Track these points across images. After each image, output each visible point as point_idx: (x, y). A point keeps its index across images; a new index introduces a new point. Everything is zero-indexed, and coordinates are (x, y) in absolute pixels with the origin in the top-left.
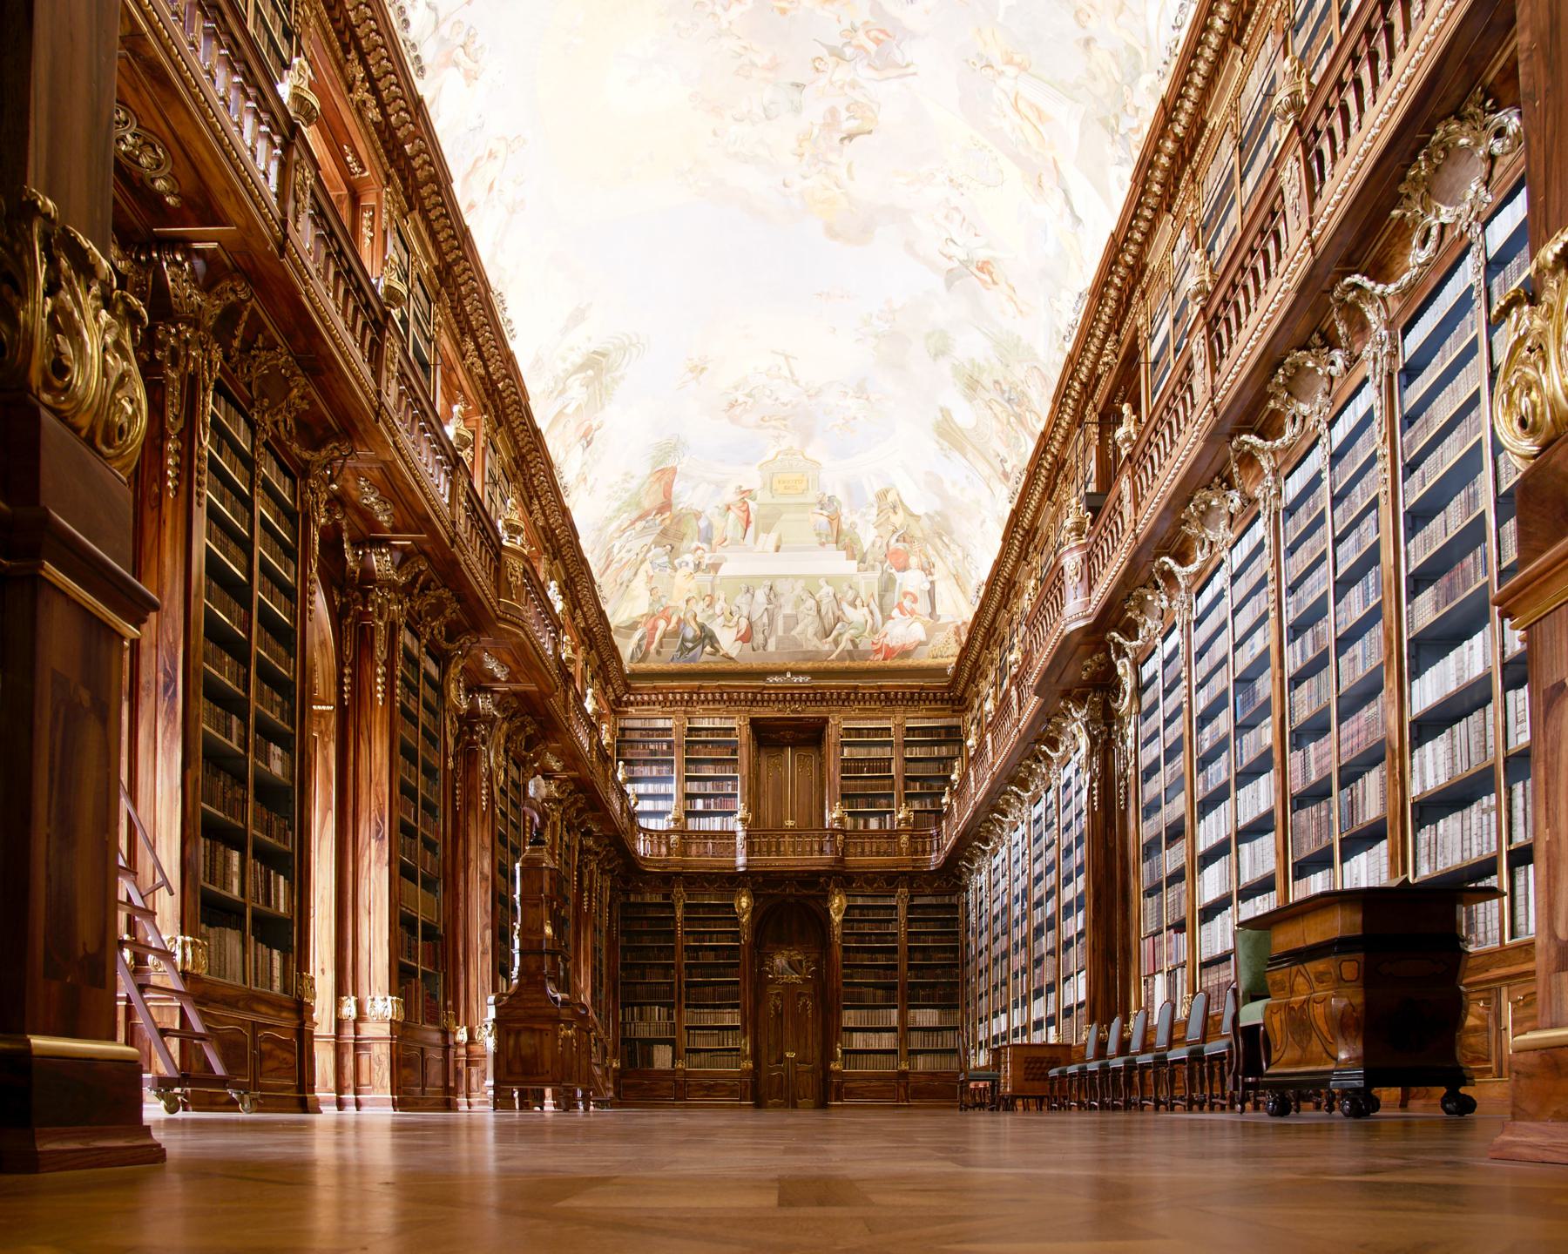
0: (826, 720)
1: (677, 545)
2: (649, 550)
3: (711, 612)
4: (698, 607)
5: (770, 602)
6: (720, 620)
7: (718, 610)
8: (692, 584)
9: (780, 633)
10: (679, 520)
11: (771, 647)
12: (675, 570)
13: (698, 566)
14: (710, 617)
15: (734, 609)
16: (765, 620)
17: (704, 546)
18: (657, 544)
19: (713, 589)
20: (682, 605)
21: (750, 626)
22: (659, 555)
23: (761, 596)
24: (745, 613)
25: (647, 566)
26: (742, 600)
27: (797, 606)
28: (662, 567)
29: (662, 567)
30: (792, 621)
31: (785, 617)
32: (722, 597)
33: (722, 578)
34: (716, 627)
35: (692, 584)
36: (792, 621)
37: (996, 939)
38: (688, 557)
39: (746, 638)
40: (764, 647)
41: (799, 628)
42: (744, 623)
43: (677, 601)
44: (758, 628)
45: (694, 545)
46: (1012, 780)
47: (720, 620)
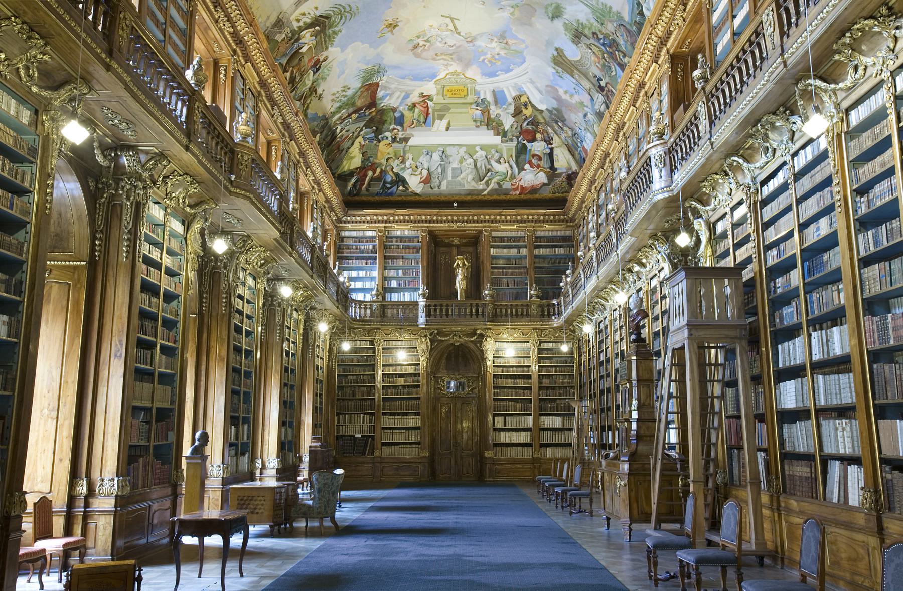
0: (481, 232)
1: (380, 127)
2: (361, 130)
4: (395, 164)
5: (442, 160)
7: (408, 164)
8: (390, 150)
9: (450, 178)
10: (382, 112)
11: (444, 187)
12: (379, 141)
13: (394, 140)
14: (402, 169)
15: (418, 164)
16: (440, 171)
17: (399, 128)
18: (366, 126)
19: (405, 152)
20: (384, 162)
21: (430, 174)
22: (368, 132)
23: (436, 157)
24: (426, 167)
26: (424, 159)
27: (461, 162)
29: (371, 140)
30: (457, 172)
31: (453, 169)
32: (411, 157)
33: (411, 147)
34: (406, 175)
36: (457, 172)
37: (602, 377)
39: (427, 181)
41: (462, 176)
42: (425, 173)
44: (434, 176)
45: (391, 127)
46: (611, 282)
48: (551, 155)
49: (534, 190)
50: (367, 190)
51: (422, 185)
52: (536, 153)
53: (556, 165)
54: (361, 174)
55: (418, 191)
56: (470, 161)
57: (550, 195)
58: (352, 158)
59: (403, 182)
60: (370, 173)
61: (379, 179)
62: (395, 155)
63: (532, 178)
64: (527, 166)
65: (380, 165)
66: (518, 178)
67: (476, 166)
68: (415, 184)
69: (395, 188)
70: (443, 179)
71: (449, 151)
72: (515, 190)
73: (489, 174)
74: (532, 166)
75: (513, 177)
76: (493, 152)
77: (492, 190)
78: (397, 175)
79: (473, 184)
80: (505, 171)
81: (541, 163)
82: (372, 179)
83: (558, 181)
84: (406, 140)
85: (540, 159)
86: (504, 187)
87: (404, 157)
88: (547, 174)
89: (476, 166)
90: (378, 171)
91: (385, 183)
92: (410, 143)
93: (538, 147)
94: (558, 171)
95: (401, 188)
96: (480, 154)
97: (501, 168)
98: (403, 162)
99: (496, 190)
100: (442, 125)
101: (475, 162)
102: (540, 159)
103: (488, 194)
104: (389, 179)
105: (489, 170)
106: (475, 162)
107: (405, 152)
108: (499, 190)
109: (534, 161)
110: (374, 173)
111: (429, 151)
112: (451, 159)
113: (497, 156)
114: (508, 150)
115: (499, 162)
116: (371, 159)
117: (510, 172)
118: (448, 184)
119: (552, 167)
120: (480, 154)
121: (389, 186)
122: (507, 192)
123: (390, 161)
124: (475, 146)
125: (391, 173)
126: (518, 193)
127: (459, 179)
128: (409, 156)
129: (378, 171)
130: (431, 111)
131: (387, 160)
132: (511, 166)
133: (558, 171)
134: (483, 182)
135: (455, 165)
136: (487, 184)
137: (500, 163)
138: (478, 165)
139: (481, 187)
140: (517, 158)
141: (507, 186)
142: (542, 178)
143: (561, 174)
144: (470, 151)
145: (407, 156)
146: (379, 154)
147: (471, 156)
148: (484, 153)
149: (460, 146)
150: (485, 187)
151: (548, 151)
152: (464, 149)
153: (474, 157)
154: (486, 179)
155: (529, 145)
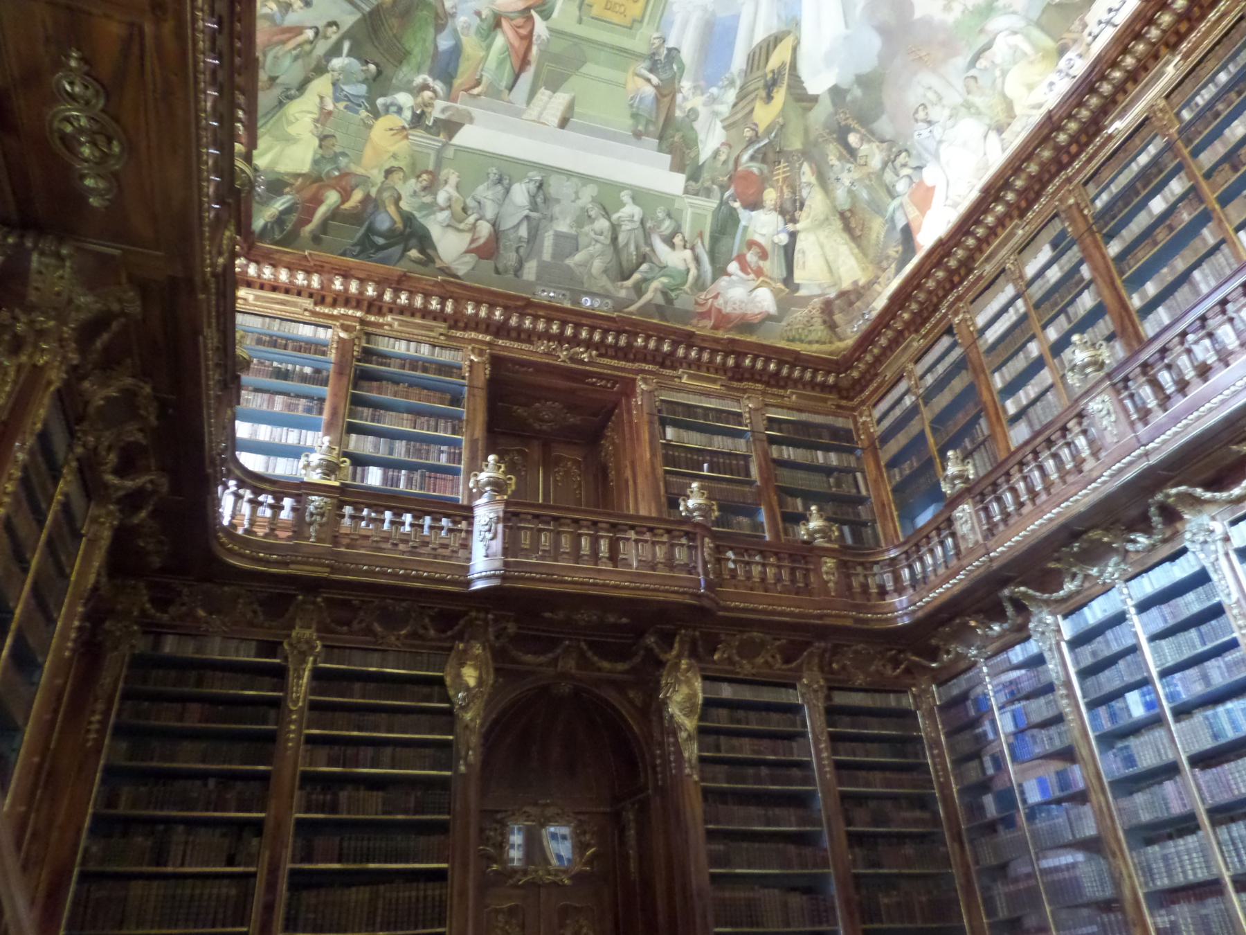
3: (428, 199)
4: (408, 188)
5: (534, 206)
6: (443, 216)
7: (441, 198)
8: (401, 146)
9: (547, 256)
11: (530, 271)
15: (471, 203)
16: (523, 232)
19: (439, 162)
20: (377, 176)
21: (497, 233)
23: (520, 194)
24: (490, 214)
25: (321, 85)
26: (486, 193)
28: (353, 103)
30: (568, 244)
31: (558, 236)
32: (453, 179)
33: (460, 149)
34: (435, 226)
35: (401, 146)
36: (568, 244)
38: (404, 99)
39: (488, 250)
40: (518, 270)
41: (579, 257)
42: (485, 229)
43: (370, 166)
47: (443, 216)
48: (789, 251)
49: (746, 325)
50: (316, 239)
51: (471, 259)
52: (757, 238)
53: (798, 277)
54: (307, 193)
55: (462, 270)
56: (603, 224)
57: (782, 344)
58: (290, 140)
59: (424, 241)
60: (332, 198)
61: (355, 218)
62: (413, 165)
63: (744, 295)
64: (733, 267)
65: (365, 181)
66: (712, 290)
67: (614, 239)
68: (451, 246)
69: (397, 250)
70: (529, 256)
71: (556, 186)
72: (705, 315)
73: (644, 267)
74: (744, 267)
75: (699, 285)
76: (661, 215)
77: (649, 303)
78: (408, 219)
79: (604, 282)
80: (682, 267)
81: (766, 265)
82: (335, 214)
83: (799, 314)
84: (450, 127)
85: (764, 255)
86: (678, 304)
87: (434, 175)
88: (776, 293)
89: (614, 239)
90: (357, 196)
91: (371, 230)
92: (458, 140)
93: (763, 225)
94: (802, 292)
95: (414, 253)
96: (630, 211)
97: (675, 258)
98: (431, 188)
99: (658, 307)
100: (553, 104)
101: (615, 228)
102: (764, 255)
103: (641, 311)
104: (383, 223)
105: (643, 258)
106: (615, 228)
107: (439, 162)
108: (666, 306)
109: (751, 257)
110: (346, 195)
111: (504, 172)
112: (556, 209)
113: (667, 226)
114: (697, 217)
115: (669, 241)
116: (343, 161)
117: (693, 272)
118: (543, 268)
119: (788, 280)
120: (630, 211)
121: (381, 241)
122: (686, 316)
123: (397, 176)
124: (622, 187)
125: (392, 209)
126: (710, 323)
127: (570, 262)
128: (451, 176)
129: (357, 196)
130: (535, 49)
131: (389, 172)
132: (697, 259)
133: (802, 292)
134: (629, 283)
135: (563, 226)
136: (639, 290)
137: (673, 246)
138: (622, 239)
139: (623, 293)
140: (715, 240)
141: (683, 301)
142: (764, 300)
143: (808, 299)
144: (608, 195)
145: (444, 173)
146: (368, 152)
147: (607, 215)
148: (637, 212)
149: (586, 179)
150: (633, 296)
151: (784, 239)
152: (589, 192)
153: (615, 217)
154: (637, 276)
155: (744, 215)
